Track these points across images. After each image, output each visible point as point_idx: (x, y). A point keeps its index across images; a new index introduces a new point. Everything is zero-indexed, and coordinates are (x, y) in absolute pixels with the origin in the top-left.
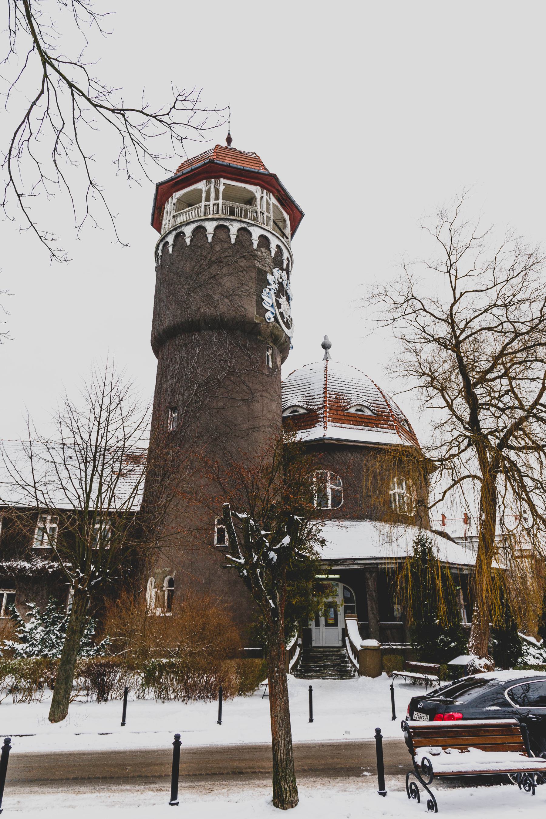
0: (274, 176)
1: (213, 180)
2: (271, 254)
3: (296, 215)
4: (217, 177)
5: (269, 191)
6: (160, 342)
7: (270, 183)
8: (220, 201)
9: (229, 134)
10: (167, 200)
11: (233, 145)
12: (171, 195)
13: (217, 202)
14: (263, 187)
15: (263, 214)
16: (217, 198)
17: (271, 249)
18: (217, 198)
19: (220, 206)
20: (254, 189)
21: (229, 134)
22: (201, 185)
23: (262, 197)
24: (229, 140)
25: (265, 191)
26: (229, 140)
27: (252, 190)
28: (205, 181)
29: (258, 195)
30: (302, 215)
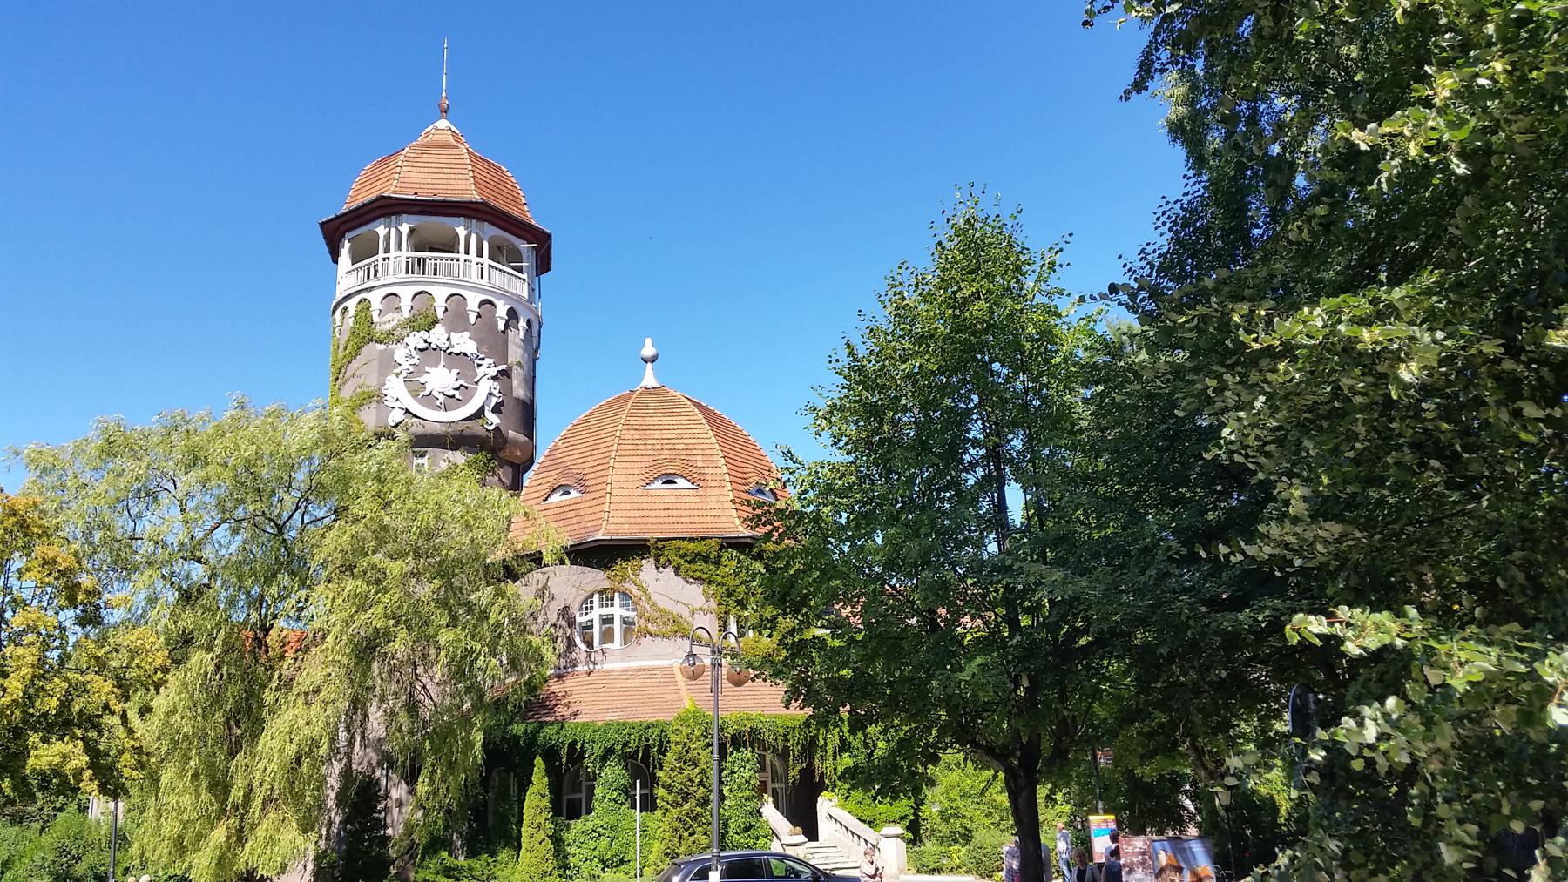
8: (485, 259)
10: (388, 215)
16: (480, 254)
18: (480, 254)
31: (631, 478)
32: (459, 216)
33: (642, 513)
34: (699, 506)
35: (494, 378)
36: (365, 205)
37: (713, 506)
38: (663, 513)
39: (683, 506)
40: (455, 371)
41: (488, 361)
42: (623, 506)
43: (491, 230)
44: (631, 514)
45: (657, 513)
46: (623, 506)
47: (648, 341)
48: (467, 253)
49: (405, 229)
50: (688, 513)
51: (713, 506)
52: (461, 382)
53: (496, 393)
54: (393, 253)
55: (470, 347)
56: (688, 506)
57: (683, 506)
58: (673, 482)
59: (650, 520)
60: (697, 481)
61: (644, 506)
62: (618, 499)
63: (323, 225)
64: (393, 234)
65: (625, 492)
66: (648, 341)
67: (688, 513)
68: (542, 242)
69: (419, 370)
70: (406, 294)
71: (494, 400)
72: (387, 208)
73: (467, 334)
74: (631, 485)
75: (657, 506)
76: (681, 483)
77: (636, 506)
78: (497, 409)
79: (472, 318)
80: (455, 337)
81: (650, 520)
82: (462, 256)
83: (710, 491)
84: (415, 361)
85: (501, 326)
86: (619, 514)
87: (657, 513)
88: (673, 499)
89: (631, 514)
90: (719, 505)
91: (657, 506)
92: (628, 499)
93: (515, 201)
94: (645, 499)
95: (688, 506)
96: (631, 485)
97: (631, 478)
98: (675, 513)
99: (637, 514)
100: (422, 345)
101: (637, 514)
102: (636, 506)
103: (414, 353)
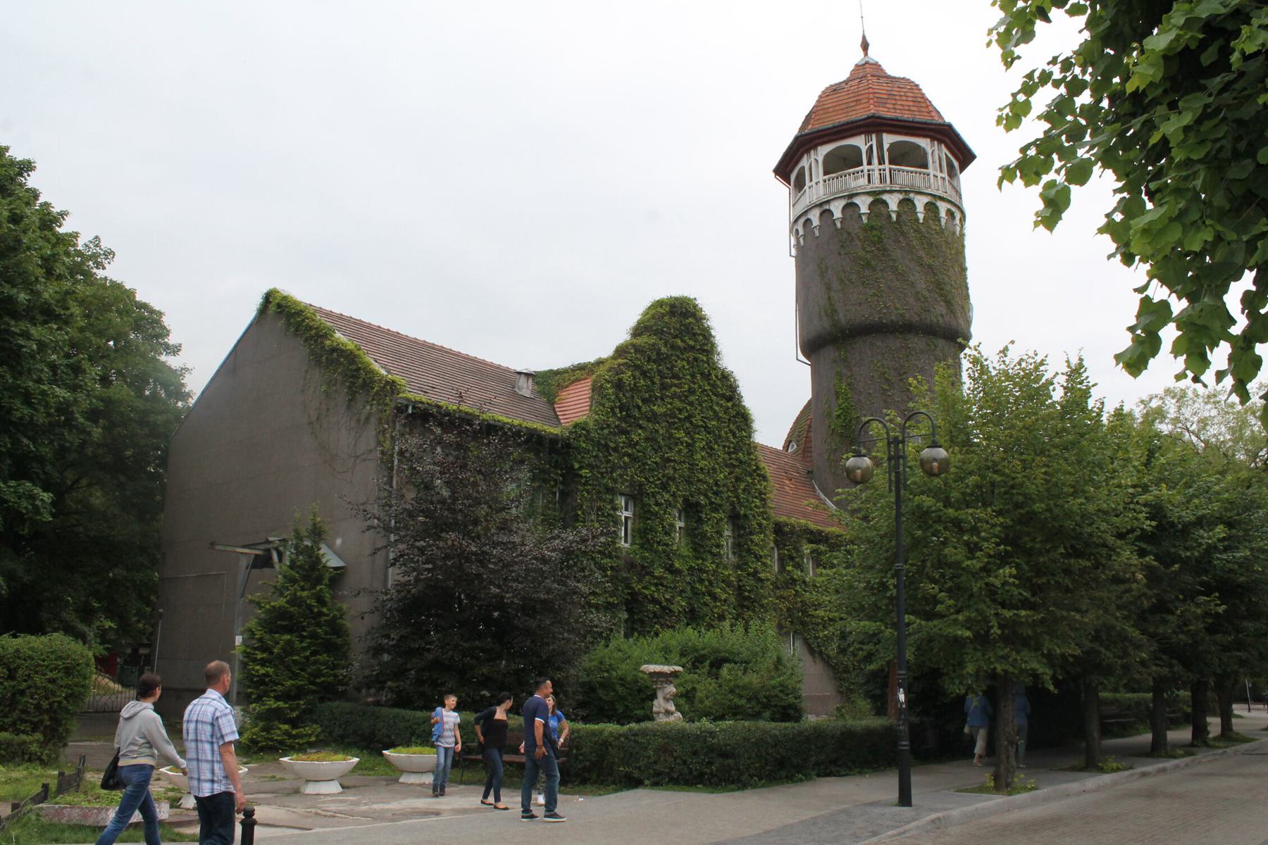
0: (950, 126)
5: (940, 141)
6: (812, 346)
7: (946, 135)
8: (887, 166)
9: (864, 37)
10: (808, 151)
11: (874, 54)
12: (815, 147)
13: (882, 167)
14: (933, 139)
18: (881, 161)
20: (924, 143)
21: (864, 37)
22: (859, 142)
24: (865, 46)
26: (865, 46)
29: (929, 152)
43: (888, 139)
48: (869, 163)
49: (820, 160)
82: (865, 167)
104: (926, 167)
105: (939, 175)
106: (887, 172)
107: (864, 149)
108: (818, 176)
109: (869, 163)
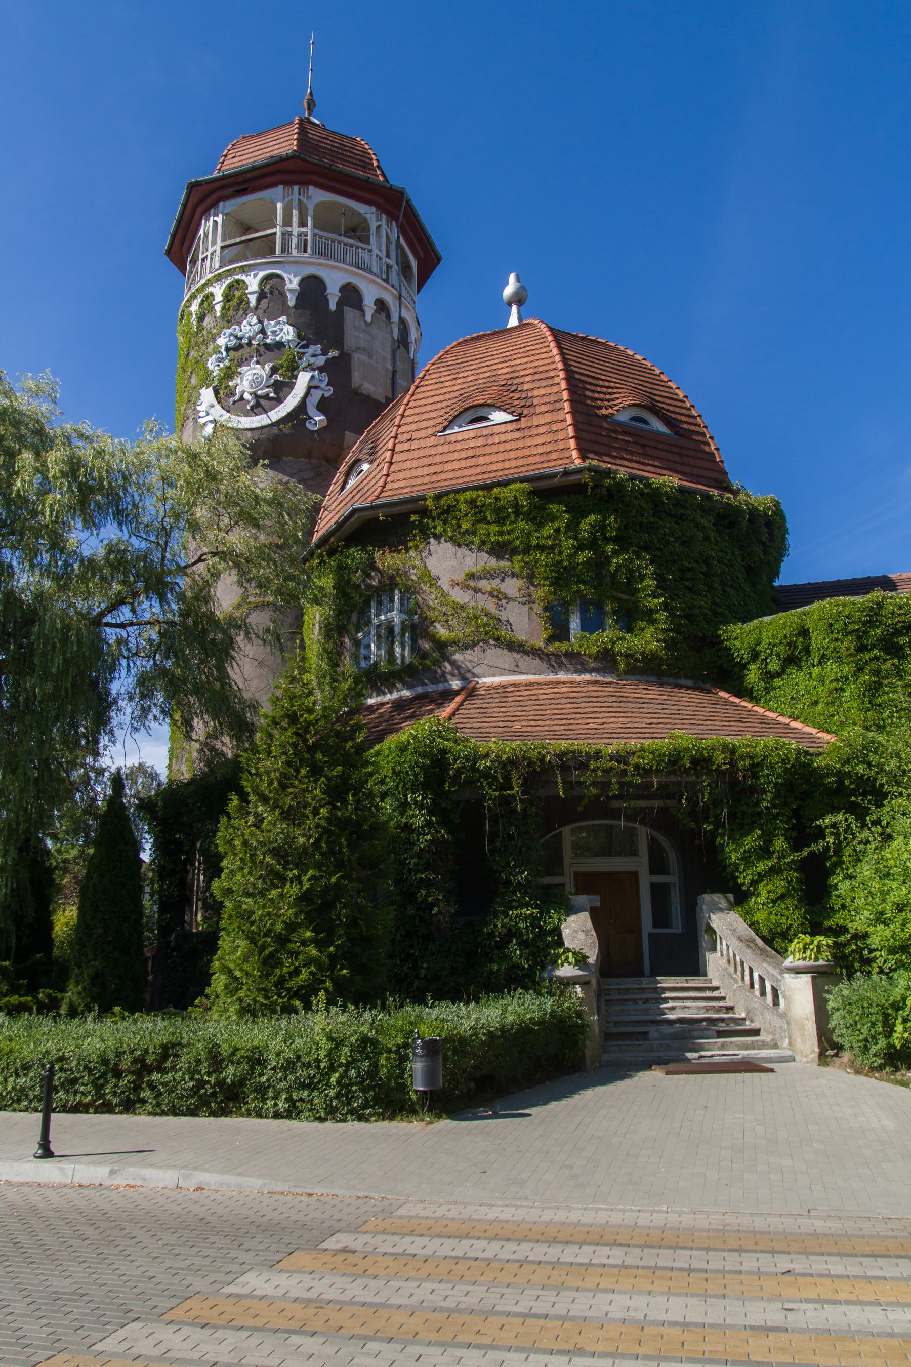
1: (296, 188)
2: (364, 316)
3: (429, 260)
4: (304, 183)
8: (308, 230)
10: (206, 212)
12: (215, 204)
13: (303, 230)
14: (381, 209)
15: (381, 259)
17: (365, 308)
18: (303, 224)
19: (309, 238)
23: (379, 227)
24: (311, 106)
25: (384, 216)
27: (362, 211)
28: (281, 187)
29: (373, 226)
30: (439, 259)
31: (424, 424)
32: (274, 185)
33: (433, 469)
34: (520, 444)
35: (321, 369)
36: (185, 205)
37: (540, 440)
38: (463, 464)
39: (494, 449)
40: (267, 367)
41: (312, 349)
42: (408, 465)
43: (317, 196)
44: (419, 472)
45: (456, 465)
46: (408, 465)
47: (512, 278)
48: (287, 222)
50: (500, 457)
51: (540, 440)
52: (277, 377)
53: (323, 385)
54: (210, 250)
55: (287, 333)
56: (501, 448)
57: (494, 449)
58: (486, 419)
59: (443, 477)
60: (521, 411)
61: (438, 459)
62: (404, 456)
63: (169, 252)
64: (212, 229)
65: (414, 445)
66: (512, 278)
67: (500, 457)
68: (393, 203)
69: (230, 373)
70: (218, 291)
71: (316, 396)
72: (204, 197)
73: (283, 319)
74: (423, 434)
75: (456, 456)
76: (498, 416)
77: (426, 461)
78: (322, 406)
79: (291, 302)
80: (270, 326)
81: (443, 477)
83: (536, 421)
84: (227, 363)
85: (333, 307)
86: (401, 476)
87: (456, 465)
88: (480, 442)
89: (419, 472)
90: (548, 438)
91: (456, 456)
92: (417, 454)
93: (366, 164)
94: (440, 449)
95: (501, 448)
96: (423, 434)
97: (424, 424)
98: (482, 460)
99: (426, 471)
100: (233, 342)
101: (426, 471)
102: (426, 461)
103: (224, 354)
104: (367, 240)
105: (385, 260)
106: (309, 238)
107: (279, 205)
108: (214, 243)
109: (287, 222)
